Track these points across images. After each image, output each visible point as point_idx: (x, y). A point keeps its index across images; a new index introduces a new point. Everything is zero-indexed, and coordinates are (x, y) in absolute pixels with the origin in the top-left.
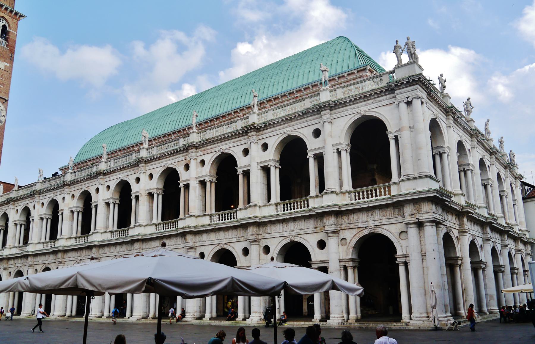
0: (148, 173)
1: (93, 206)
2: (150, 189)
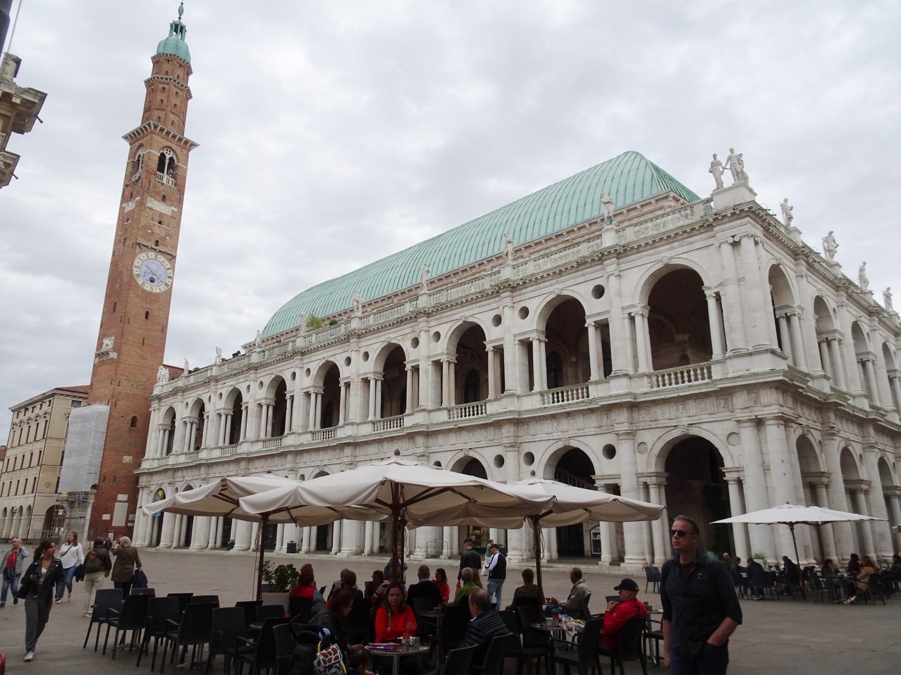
0: (363, 350)
1: (288, 397)
2: (366, 374)
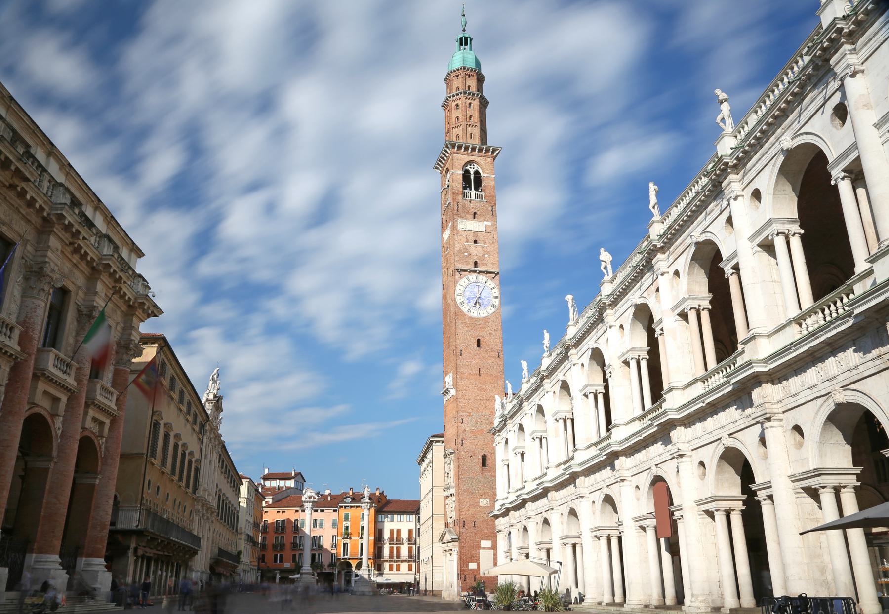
2: (623, 355)
